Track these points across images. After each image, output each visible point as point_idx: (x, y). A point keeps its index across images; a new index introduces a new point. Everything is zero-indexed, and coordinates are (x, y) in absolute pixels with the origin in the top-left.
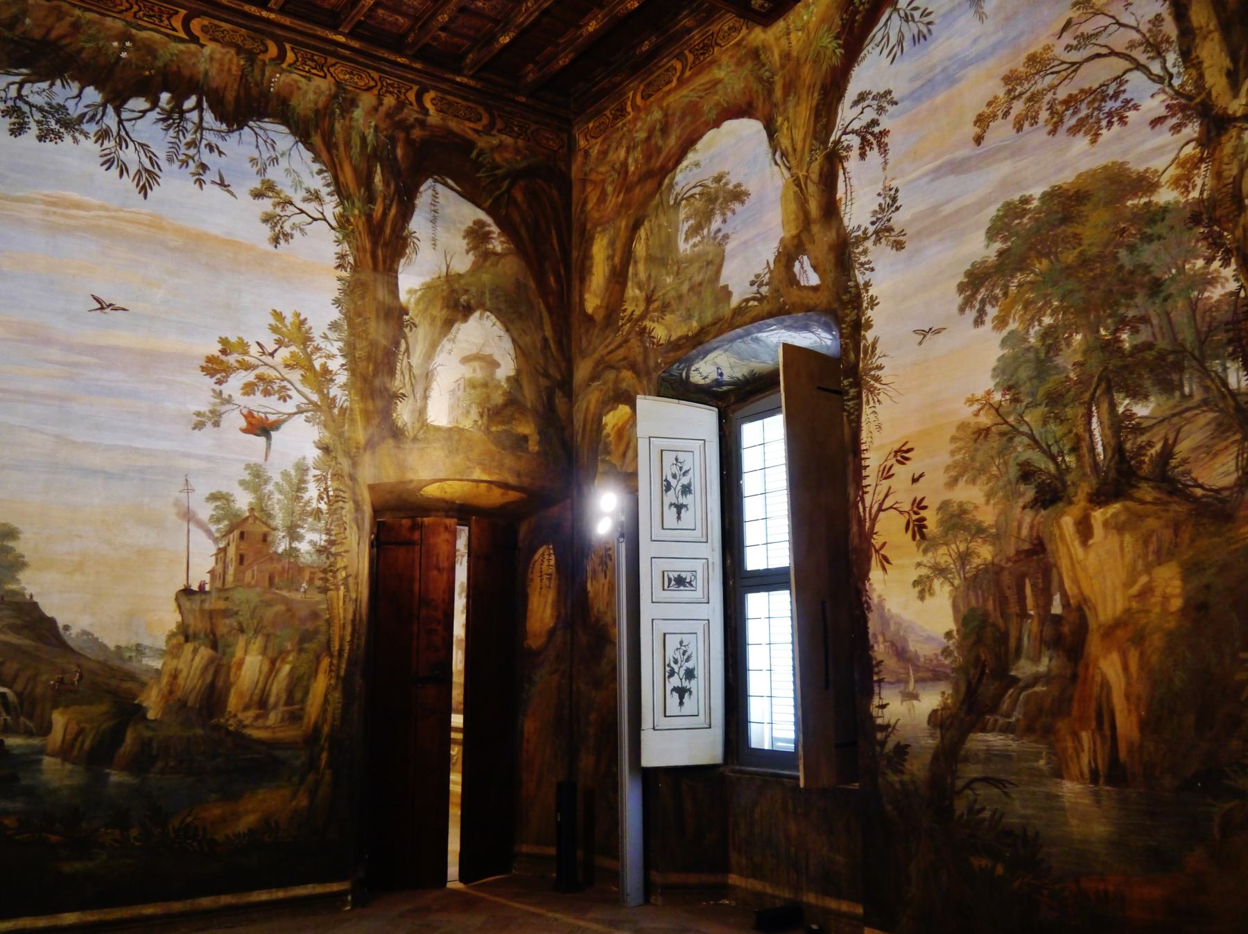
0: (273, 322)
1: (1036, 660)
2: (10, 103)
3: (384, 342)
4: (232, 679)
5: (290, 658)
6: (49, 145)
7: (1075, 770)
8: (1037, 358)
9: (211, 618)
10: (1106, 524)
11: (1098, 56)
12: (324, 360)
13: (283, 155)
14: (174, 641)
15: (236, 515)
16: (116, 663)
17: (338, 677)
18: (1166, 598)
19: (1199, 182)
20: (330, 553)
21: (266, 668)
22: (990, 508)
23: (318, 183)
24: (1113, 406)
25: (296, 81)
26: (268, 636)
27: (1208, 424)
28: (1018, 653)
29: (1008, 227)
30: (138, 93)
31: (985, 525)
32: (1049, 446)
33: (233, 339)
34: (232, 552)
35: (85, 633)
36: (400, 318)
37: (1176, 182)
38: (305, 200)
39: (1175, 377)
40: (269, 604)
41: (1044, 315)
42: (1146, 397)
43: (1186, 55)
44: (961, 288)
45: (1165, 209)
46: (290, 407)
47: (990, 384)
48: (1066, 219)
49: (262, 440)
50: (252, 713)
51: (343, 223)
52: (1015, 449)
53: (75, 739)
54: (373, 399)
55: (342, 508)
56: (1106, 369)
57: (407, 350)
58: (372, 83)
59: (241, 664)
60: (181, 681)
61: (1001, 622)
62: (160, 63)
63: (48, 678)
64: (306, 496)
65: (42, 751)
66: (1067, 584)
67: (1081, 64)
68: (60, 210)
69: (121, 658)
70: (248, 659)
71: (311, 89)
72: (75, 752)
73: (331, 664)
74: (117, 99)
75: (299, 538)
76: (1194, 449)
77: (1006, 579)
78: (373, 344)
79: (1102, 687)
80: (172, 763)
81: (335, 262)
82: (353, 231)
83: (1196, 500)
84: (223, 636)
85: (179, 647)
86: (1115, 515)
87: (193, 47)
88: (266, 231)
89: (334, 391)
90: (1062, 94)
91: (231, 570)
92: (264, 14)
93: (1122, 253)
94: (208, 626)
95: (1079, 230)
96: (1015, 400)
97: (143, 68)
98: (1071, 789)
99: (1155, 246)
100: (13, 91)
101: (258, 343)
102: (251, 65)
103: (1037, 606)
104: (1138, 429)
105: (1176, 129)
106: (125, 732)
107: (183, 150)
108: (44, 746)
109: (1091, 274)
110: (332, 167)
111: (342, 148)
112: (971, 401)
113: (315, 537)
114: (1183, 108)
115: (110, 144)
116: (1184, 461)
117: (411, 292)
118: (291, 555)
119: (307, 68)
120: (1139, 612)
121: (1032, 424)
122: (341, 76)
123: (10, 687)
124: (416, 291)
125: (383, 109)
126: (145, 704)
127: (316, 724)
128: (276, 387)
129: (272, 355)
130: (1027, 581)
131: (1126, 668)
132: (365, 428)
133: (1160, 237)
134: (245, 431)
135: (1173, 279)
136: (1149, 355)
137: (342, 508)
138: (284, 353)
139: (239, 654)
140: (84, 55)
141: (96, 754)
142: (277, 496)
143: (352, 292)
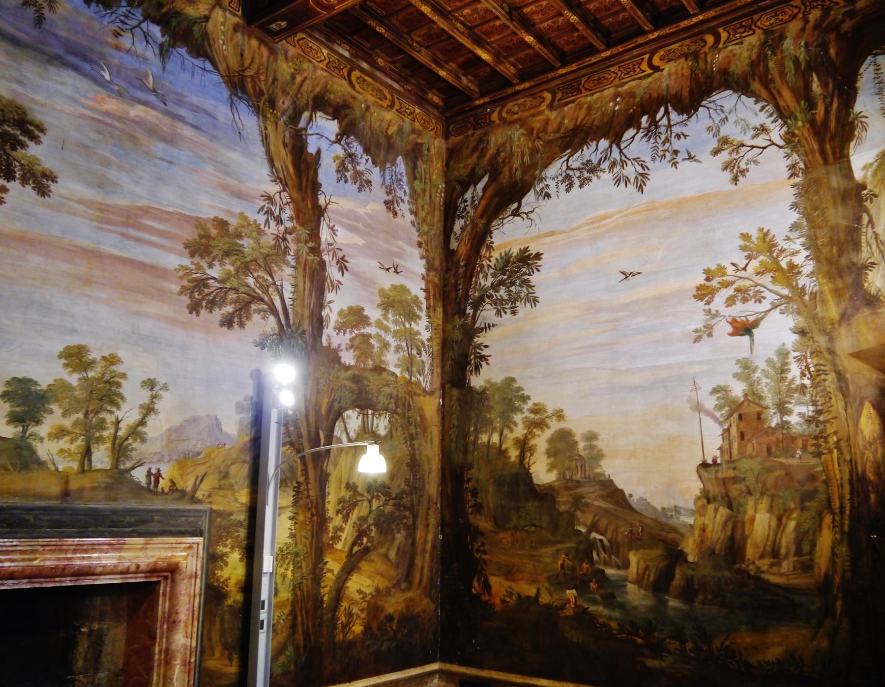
0: (742, 243)
2: (564, 174)
3: (844, 223)
4: (747, 532)
5: (795, 515)
6: (586, 188)
9: (724, 484)
12: (789, 258)
13: (730, 113)
14: (700, 503)
15: (734, 402)
16: (664, 520)
17: (842, 532)
20: (819, 421)
21: (774, 523)
23: (763, 118)
25: (731, 51)
26: (772, 497)
30: (627, 128)
33: (713, 267)
34: (734, 431)
35: (642, 499)
36: (858, 195)
38: (754, 137)
40: (769, 470)
46: (765, 306)
49: (746, 338)
50: (767, 561)
51: (790, 140)
53: (644, 573)
54: (841, 276)
55: (825, 380)
57: (871, 221)
58: (796, 11)
59: (752, 520)
60: (708, 533)
62: (638, 100)
63: (624, 530)
64: (790, 376)
65: (626, 579)
68: (595, 225)
69: (666, 516)
70: (758, 516)
71: (740, 50)
72: (645, 582)
73: (834, 520)
74: (616, 139)
75: (789, 412)
78: (834, 229)
80: (710, 597)
81: (786, 173)
82: (799, 141)
84: (735, 498)
85: (704, 507)
87: (656, 75)
88: (728, 175)
89: (802, 281)
91: (735, 446)
92: (695, 20)
94: (724, 491)
97: (629, 109)
100: (564, 167)
101: (733, 264)
102: (697, 61)
106: (674, 570)
107: (661, 148)
108: (627, 576)
110: (773, 99)
111: (778, 79)
113: (803, 409)
115: (617, 169)
117: (866, 168)
118: (783, 428)
119: (738, 36)
122: (767, 24)
123: (604, 536)
124: (871, 165)
125: (810, 26)
126: (685, 550)
127: (826, 574)
128: (751, 293)
129: (744, 269)
132: (837, 305)
134: (732, 334)
137: (825, 380)
138: (754, 264)
139: (750, 512)
140: (596, 123)
141: (660, 585)
142: (765, 380)
143: (807, 192)
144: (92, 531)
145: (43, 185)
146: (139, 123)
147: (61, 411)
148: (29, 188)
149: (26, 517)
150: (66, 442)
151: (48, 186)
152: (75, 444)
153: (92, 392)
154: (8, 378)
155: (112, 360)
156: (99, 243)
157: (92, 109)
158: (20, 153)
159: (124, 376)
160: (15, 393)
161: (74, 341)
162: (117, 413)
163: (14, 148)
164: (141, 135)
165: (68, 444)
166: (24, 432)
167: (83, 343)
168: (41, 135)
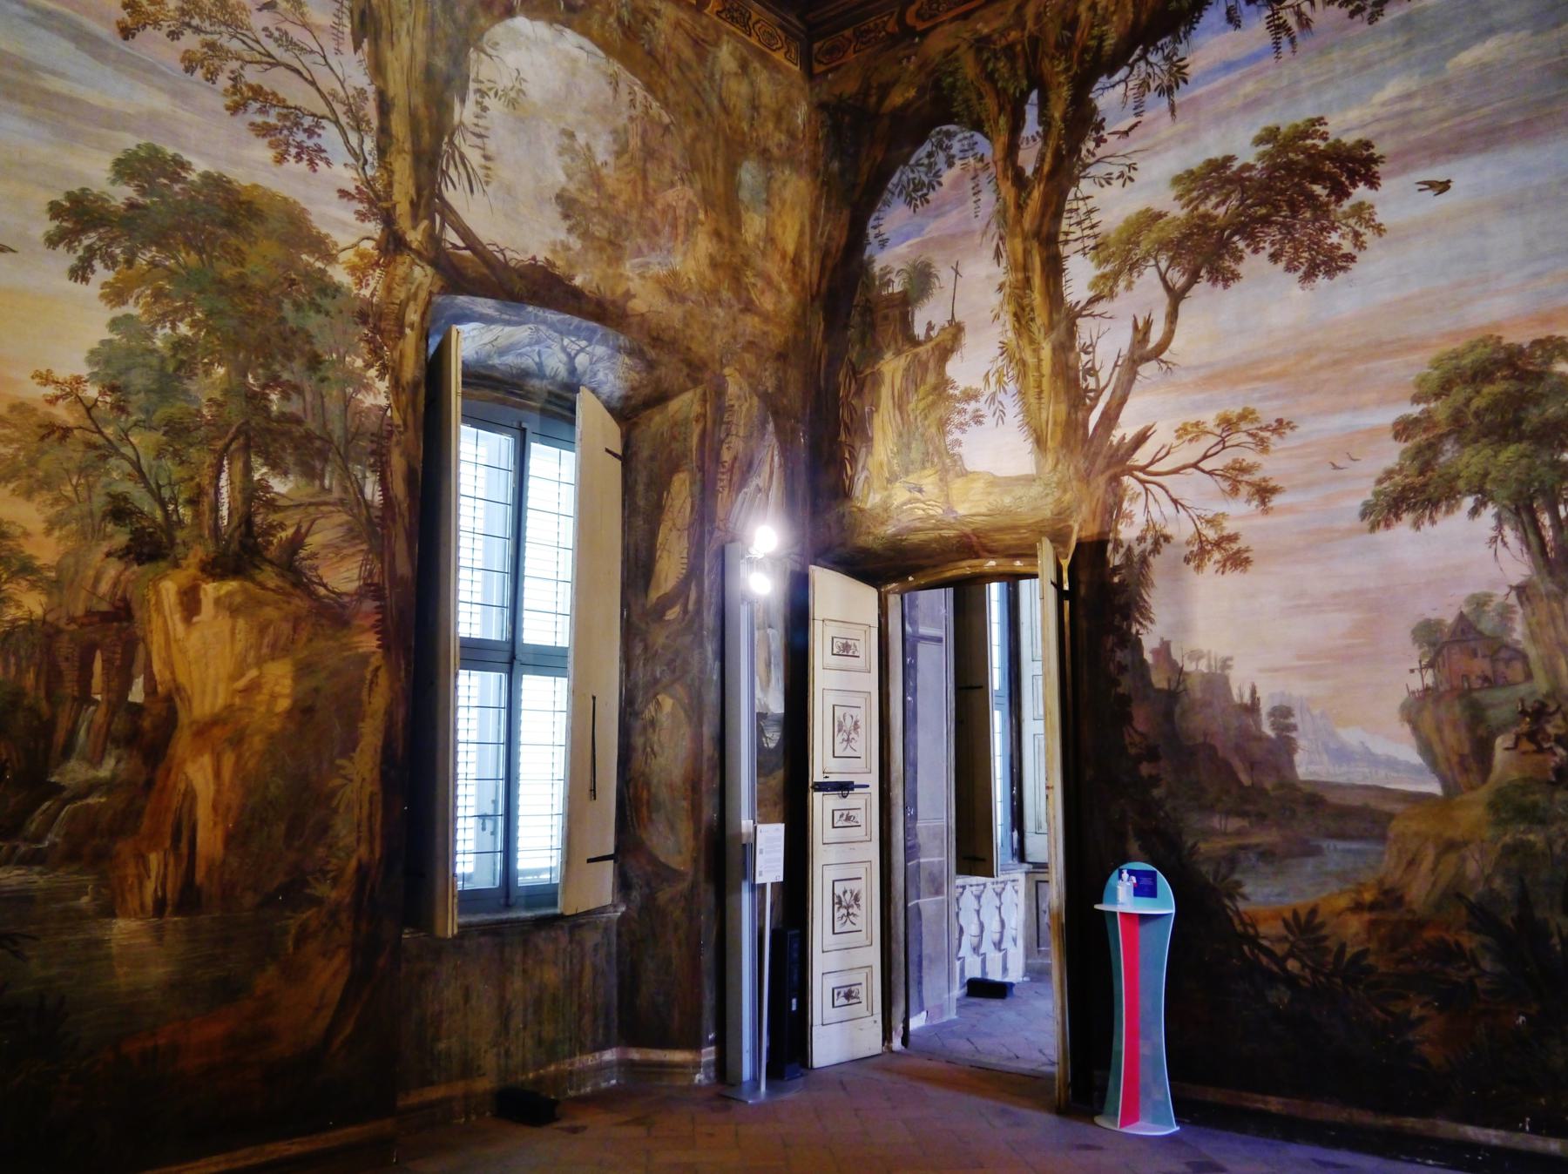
1: (96, 761)
7: (133, 903)
8: (162, 369)
10: (217, 602)
11: (300, 73)
18: (274, 697)
19: (372, 283)
22: (52, 540)
24: (248, 470)
27: (341, 525)
28: (67, 751)
29: (151, 180)
31: (38, 563)
32: (159, 487)
37: (353, 269)
39: (318, 464)
41: (181, 320)
42: (285, 473)
43: (382, 151)
44: (55, 210)
45: (336, 290)
47: (84, 371)
48: (229, 224)
52: (108, 473)
56: (247, 423)
61: (44, 706)
66: (157, 666)
67: (277, 64)
76: (325, 546)
77: (64, 647)
79: (185, 795)
83: (319, 598)
86: (230, 594)
90: (252, 75)
93: (287, 305)
95: (245, 247)
96: (120, 408)
98: (124, 930)
99: (321, 319)
103: (107, 689)
104: (272, 505)
105: (362, 216)
109: (250, 307)
112: (45, 379)
114: (371, 202)
116: (313, 556)
120: (241, 709)
121: (141, 451)
130: (98, 654)
131: (217, 774)
133: (327, 314)
135: (333, 362)
136: (298, 431)
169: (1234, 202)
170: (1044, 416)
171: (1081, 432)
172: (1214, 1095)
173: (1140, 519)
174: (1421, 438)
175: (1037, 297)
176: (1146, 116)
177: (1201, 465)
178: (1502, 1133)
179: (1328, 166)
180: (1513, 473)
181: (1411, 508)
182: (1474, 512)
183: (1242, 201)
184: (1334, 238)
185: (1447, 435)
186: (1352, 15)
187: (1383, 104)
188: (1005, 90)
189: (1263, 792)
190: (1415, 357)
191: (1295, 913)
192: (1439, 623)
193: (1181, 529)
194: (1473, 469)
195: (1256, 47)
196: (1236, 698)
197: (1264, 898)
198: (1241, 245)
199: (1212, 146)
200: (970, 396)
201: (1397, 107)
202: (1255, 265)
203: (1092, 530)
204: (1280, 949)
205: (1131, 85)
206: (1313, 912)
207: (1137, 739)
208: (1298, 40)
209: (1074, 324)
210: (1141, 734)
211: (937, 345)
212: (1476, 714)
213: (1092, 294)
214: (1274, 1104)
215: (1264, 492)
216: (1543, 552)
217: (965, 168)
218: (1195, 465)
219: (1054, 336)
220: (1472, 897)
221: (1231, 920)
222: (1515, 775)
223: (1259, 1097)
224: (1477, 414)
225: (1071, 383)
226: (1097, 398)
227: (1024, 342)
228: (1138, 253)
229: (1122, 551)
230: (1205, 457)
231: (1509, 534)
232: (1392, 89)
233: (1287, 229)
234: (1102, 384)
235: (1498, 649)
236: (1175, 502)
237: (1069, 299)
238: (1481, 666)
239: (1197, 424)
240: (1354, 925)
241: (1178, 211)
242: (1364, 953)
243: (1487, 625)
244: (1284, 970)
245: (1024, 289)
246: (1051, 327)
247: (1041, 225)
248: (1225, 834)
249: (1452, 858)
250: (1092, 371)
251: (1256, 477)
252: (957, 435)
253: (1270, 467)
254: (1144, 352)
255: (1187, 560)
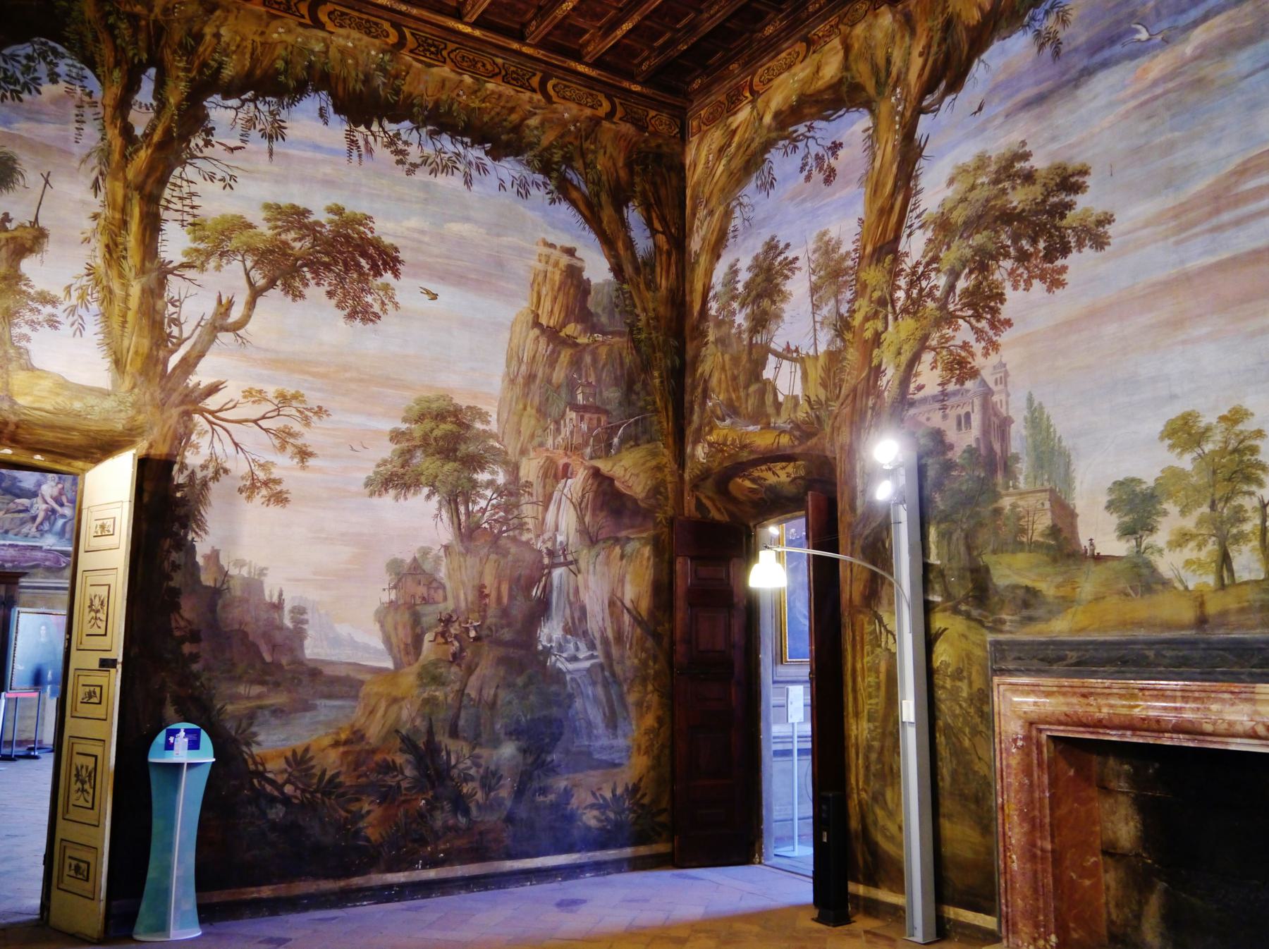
144: (1223, 673)
145: (1100, 236)
146: (1203, 54)
147: (1178, 509)
148: (1086, 250)
149: (1147, 652)
150: (1192, 550)
151: (1106, 233)
152: (1205, 551)
153: (1214, 472)
154: (1109, 485)
155: (1235, 417)
156: (1182, 262)
157: (1134, 96)
158: (1070, 215)
159: (1259, 434)
160: (1120, 500)
161: (1174, 411)
162: (1260, 492)
163: (1063, 216)
164: (1208, 69)
165: (1195, 552)
166: (1138, 545)
167: (1188, 409)
168: (1086, 179)
169: (307, 243)
170: (126, 343)
171: (160, 367)
172: (218, 897)
173: (205, 451)
174: (405, 445)
175: (132, 239)
176: (248, 146)
177: (260, 422)
178: (406, 873)
179: (371, 250)
180: (450, 479)
181: (395, 487)
182: (428, 497)
183: (313, 246)
184: (369, 299)
185: (419, 447)
186: (398, 162)
187: (408, 229)
188: (123, 50)
189: (279, 666)
190: (407, 394)
191: (294, 752)
192: (402, 561)
193: (239, 466)
194: (430, 471)
195: (336, 146)
196: (267, 598)
197: (272, 743)
198: (309, 276)
199: (294, 195)
200: (45, 299)
201: (416, 235)
202: (316, 292)
203: (161, 450)
204: (280, 779)
205: (240, 115)
206: (307, 750)
207: (182, 624)
208: (364, 157)
209: (165, 277)
210: (189, 622)
211: (13, 238)
212: (416, 619)
213: (185, 260)
214: (266, 892)
215: (304, 454)
216: (460, 529)
217: (69, 92)
218: (255, 422)
219: (144, 279)
220: (404, 732)
221: (245, 761)
222: (432, 657)
223: (254, 889)
224: (435, 439)
225: (158, 328)
226: (179, 345)
227: (113, 273)
228: (229, 246)
229: (186, 473)
230: (264, 418)
231: (444, 513)
232: (414, 223)
233: (342, 280)
234: (185, 335)
235: (432, 582)
236: (236, 445)
237: (162, 255)
238: (422, 590)
239: (260, 392)
240: (333, 756)
241: (265, 229)
242: (338, 774)
243: (427, 567)
244: (282, 793)
245: (120, 229)
246: (142, 271)
247: (144, 182)
248: (248, 698)
249: (395, 708)
250: (176, 322)
251: (299, 442)
252: (26, 330)
253: (310, 437)
254: (221, 323)
255: (240, 491)
